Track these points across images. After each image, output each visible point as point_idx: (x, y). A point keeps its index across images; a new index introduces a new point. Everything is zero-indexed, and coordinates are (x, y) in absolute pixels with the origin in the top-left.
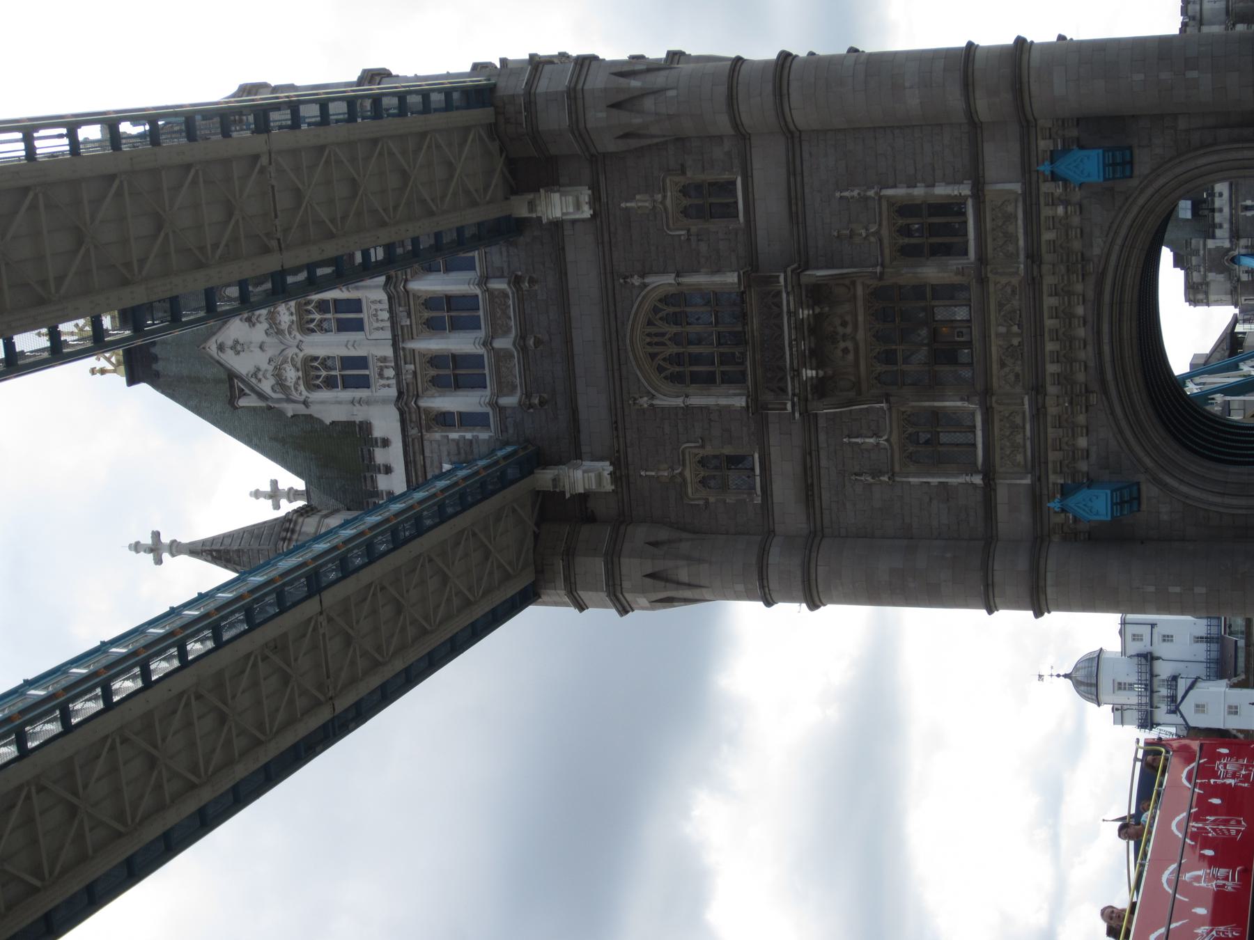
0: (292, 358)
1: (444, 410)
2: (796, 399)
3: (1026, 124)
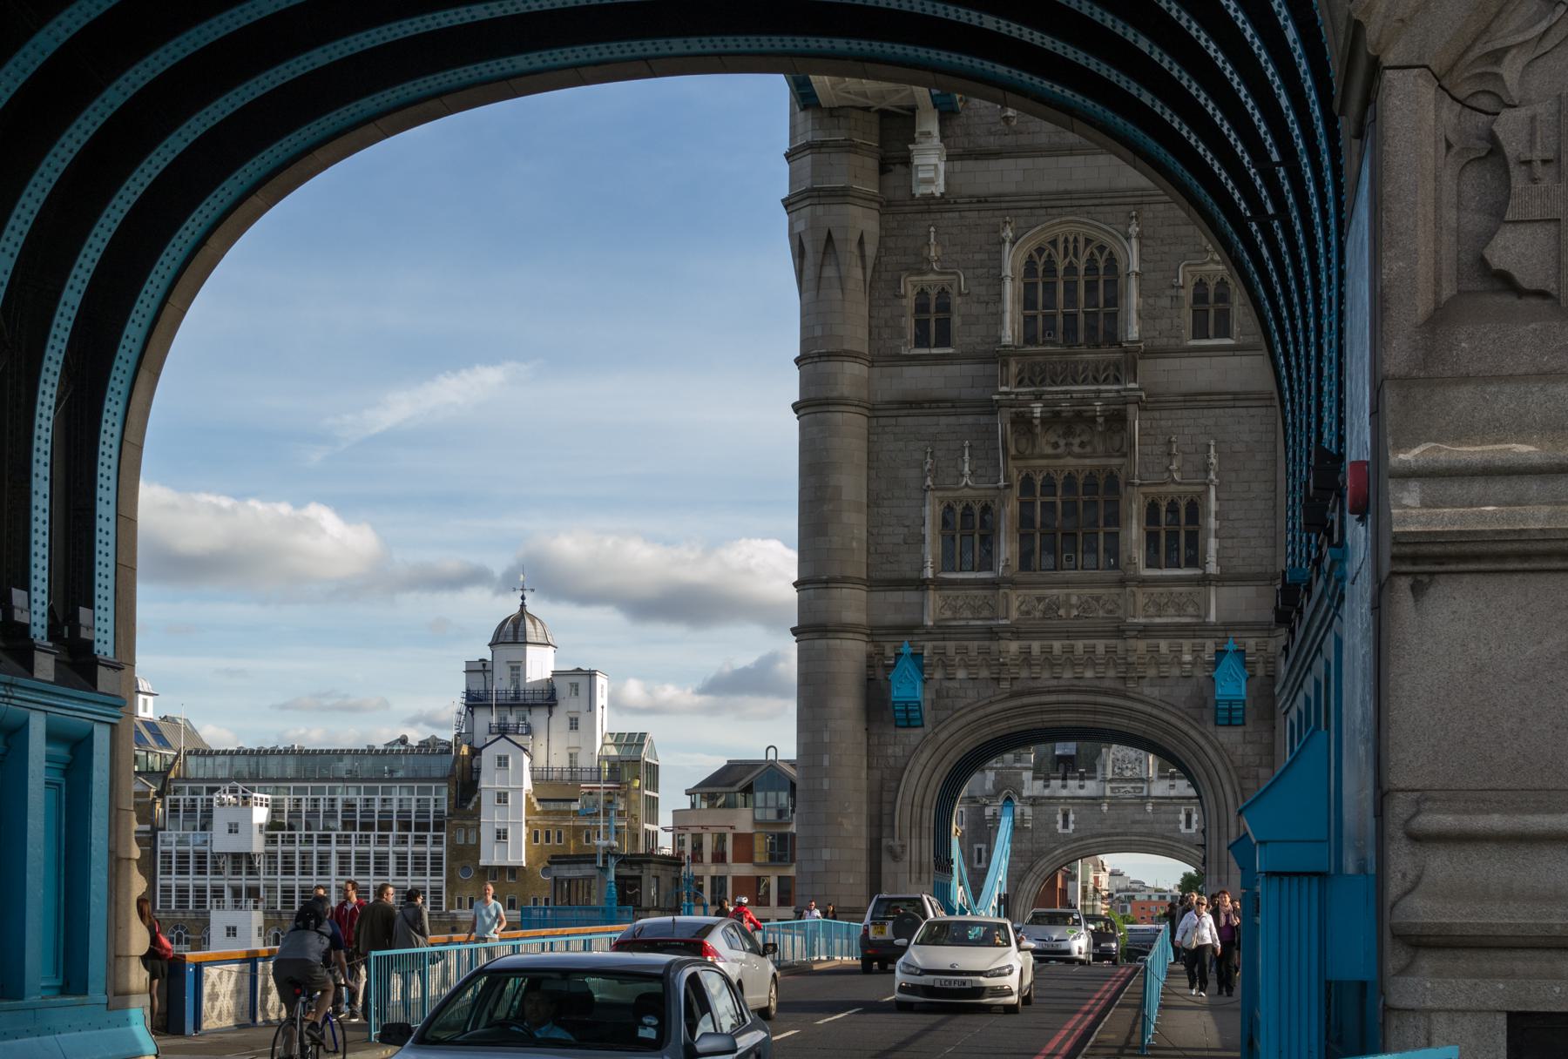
2: (1013, 396)
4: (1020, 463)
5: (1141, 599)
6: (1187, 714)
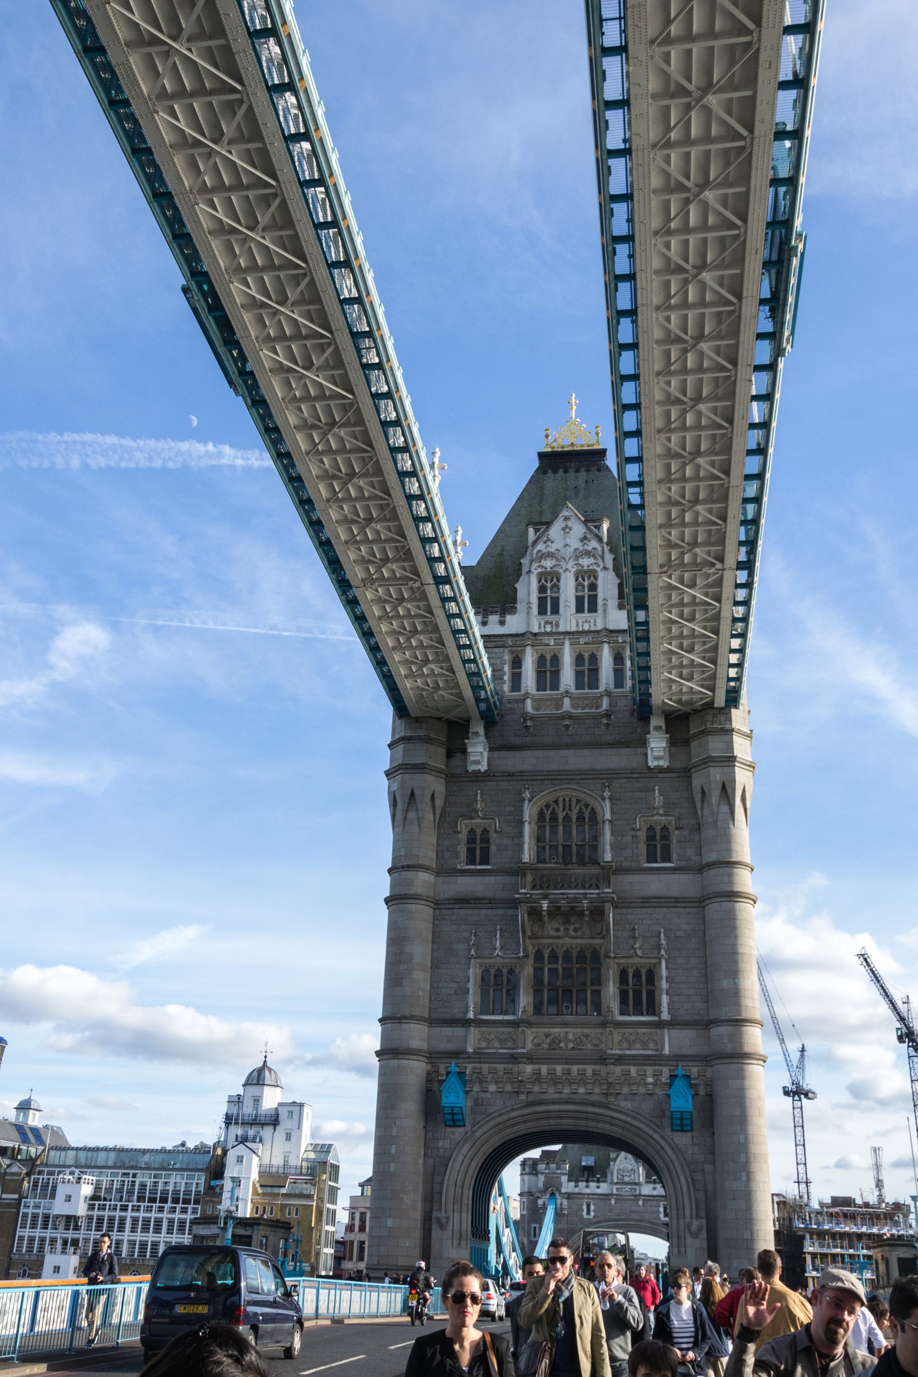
3: (707, 1060)
5: (617, 1035)
6: (651, 1121)
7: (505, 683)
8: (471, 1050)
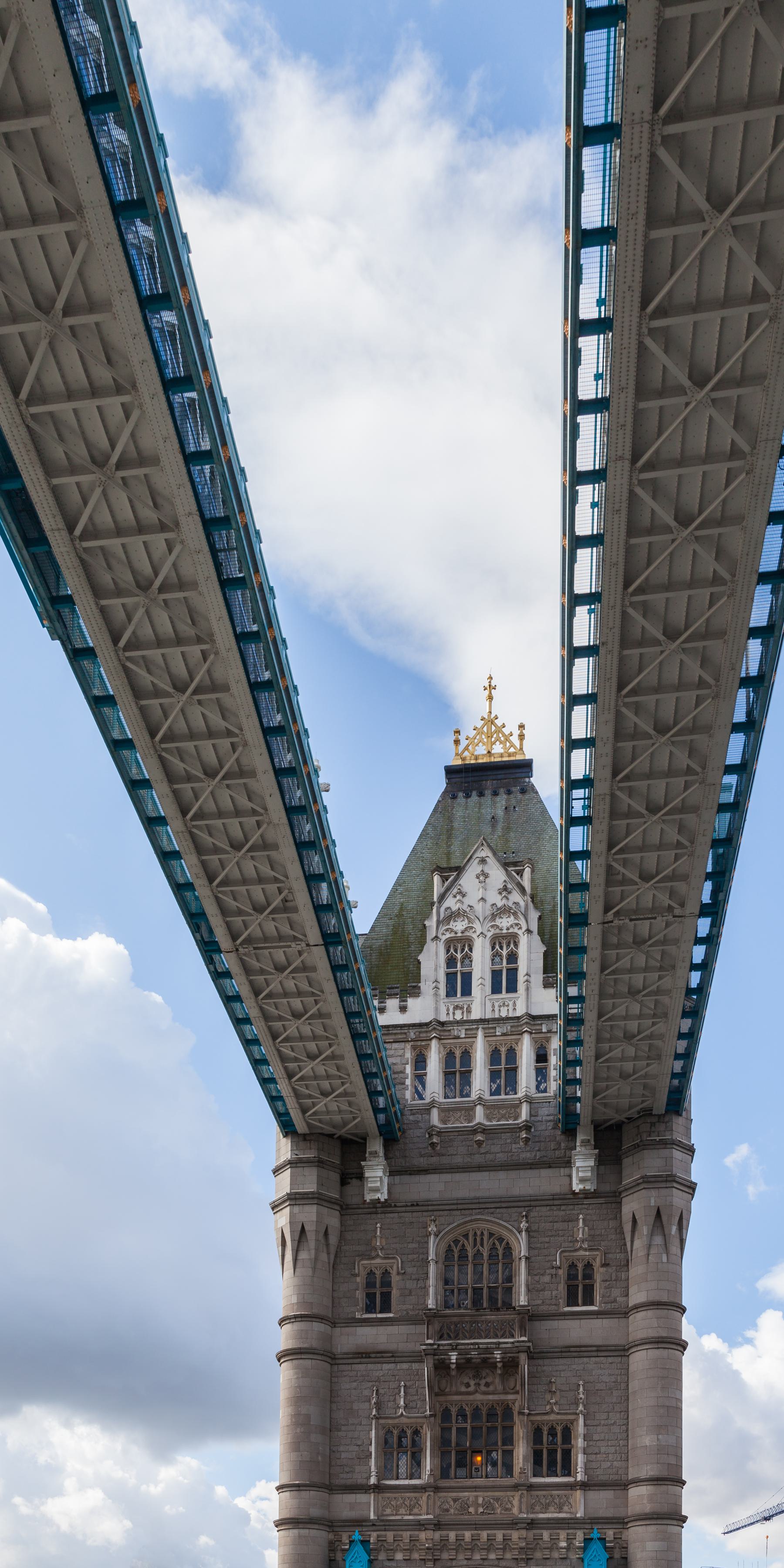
0: (472, 928)
1: (428, 1062)
4: (442, 1398)
7: (406, 1089)
8: (372, 1516)
